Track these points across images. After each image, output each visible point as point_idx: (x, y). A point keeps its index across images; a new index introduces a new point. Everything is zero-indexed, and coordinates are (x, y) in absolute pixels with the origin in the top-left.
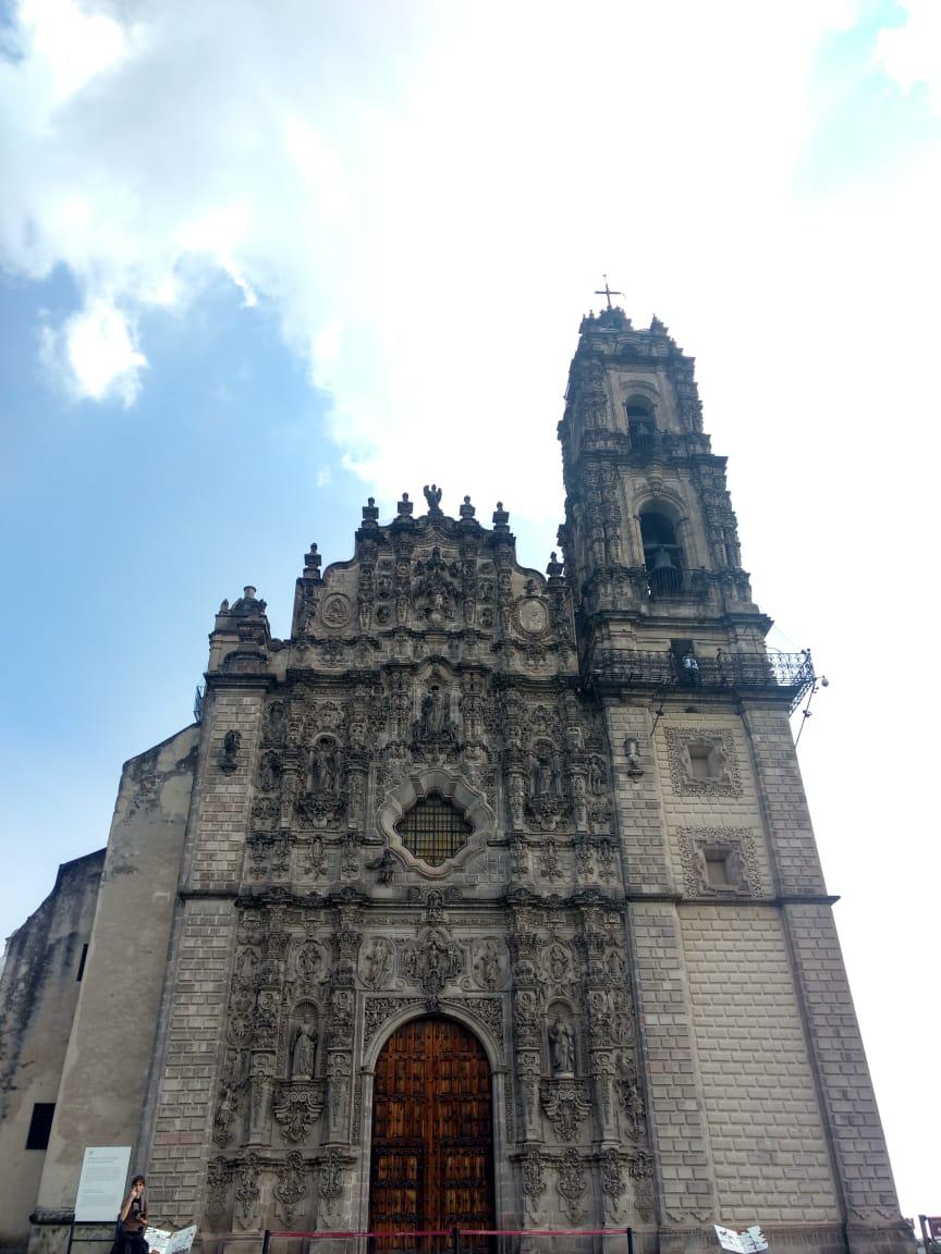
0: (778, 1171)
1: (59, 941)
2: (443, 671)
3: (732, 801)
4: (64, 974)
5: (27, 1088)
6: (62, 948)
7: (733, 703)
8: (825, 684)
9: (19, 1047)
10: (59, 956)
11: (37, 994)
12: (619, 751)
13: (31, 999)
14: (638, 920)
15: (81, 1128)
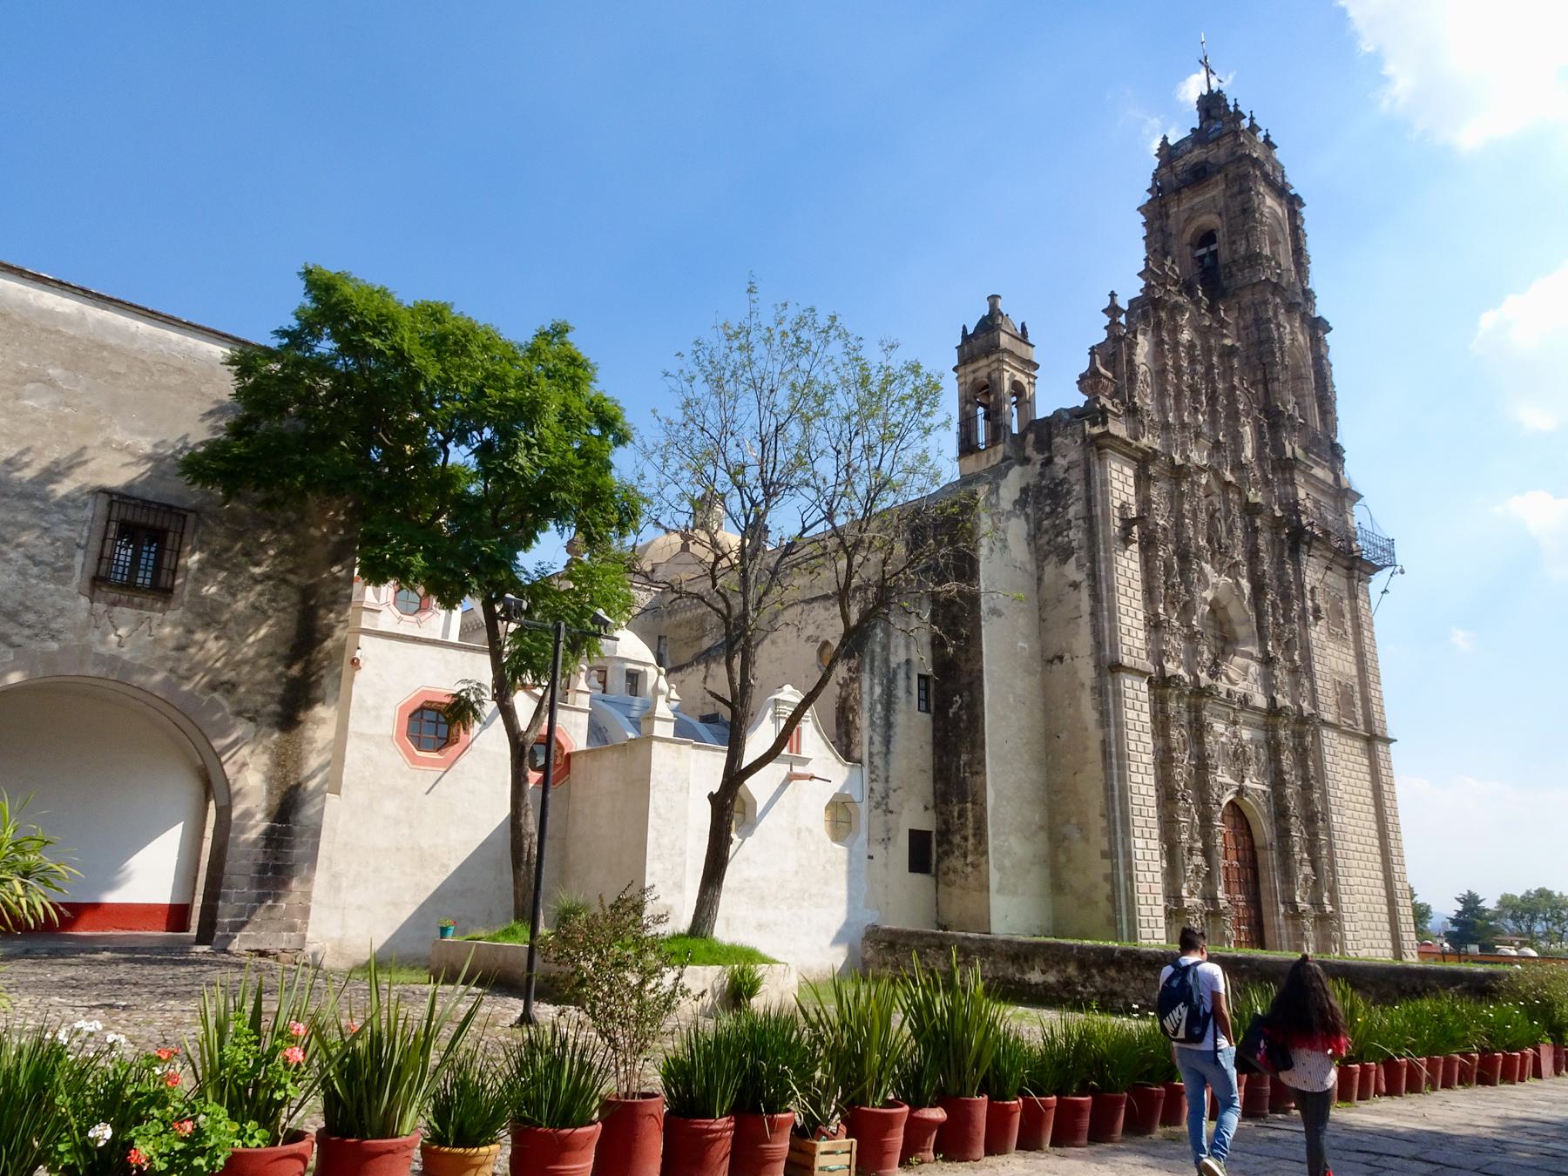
0: (1373, 925)
1: (899, 665)
2: (1213, 482)
3: (1345, 650)
4: (909, 702)
5: (900, 813)
6: (901, 675)
7: (1346, 568)
8: (1402, 572)
9: (887, 770)
10: (901, 683)
11: (892, 719)
12: (1308, 595)
13: (889, 725)
14: (1326, 741)
15: (1007, 863)
